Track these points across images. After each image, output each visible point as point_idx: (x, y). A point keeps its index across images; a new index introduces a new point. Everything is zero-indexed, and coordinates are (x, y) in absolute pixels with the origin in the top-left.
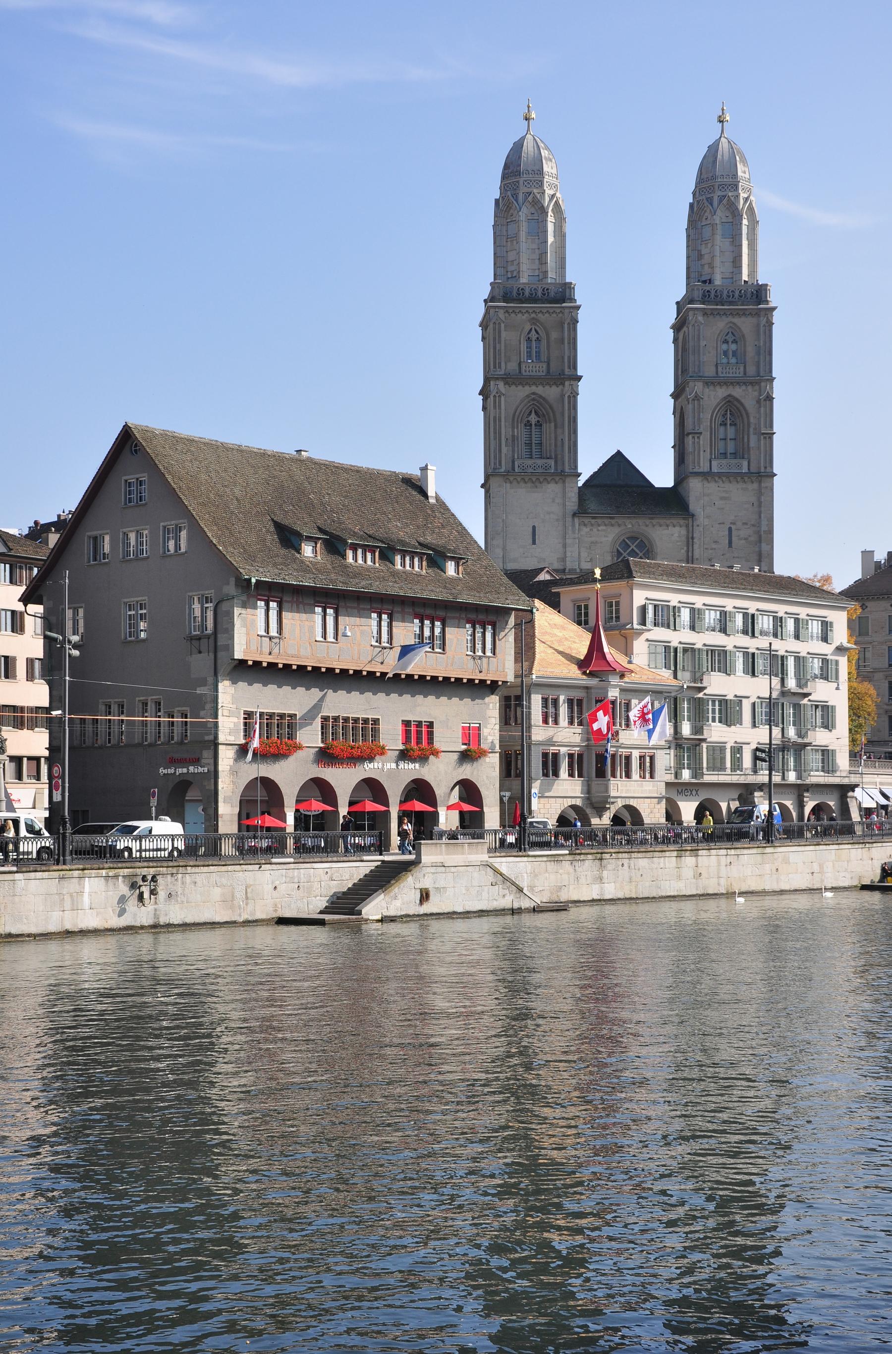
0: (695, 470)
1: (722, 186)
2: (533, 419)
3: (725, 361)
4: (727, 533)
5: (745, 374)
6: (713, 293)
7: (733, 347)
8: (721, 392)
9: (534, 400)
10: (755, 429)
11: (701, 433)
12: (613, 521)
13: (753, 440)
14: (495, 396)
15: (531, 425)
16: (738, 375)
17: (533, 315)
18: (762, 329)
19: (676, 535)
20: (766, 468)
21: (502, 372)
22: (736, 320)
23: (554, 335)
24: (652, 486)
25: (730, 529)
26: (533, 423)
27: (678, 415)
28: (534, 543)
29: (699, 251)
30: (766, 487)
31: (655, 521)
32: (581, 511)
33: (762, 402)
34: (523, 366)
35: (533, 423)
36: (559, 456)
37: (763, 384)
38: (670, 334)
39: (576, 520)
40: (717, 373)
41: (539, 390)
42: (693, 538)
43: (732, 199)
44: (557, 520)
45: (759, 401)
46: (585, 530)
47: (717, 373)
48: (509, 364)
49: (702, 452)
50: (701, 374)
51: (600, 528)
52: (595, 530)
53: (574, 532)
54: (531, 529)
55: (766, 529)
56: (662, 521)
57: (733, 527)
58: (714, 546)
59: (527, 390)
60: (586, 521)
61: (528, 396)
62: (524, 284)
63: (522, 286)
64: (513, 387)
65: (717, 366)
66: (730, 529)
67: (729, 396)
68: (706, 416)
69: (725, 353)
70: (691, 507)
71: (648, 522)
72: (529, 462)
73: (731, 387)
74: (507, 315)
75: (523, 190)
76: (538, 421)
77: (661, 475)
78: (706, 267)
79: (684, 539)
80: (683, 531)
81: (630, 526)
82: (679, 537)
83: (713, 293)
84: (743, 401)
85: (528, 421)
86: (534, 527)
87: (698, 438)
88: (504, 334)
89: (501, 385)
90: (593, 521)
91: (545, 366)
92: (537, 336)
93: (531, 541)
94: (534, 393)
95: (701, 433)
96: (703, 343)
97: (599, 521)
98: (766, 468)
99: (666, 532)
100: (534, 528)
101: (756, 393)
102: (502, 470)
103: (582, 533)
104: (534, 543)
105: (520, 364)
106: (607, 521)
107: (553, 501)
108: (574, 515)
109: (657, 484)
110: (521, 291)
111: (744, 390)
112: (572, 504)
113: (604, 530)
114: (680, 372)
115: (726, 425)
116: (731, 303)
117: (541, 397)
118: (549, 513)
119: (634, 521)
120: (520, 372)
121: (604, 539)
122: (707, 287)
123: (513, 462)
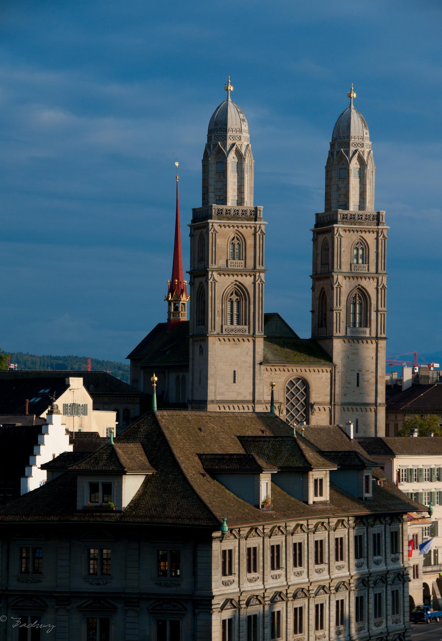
0: (337, 335)
1: (356, 145)
2: (234, 297)
3: (355, 261)
4: (356, 377)
5: (368, 270)
6: (349, 216)
7: (360, 252)
8: (354, 283)
9: (235, 285)
10: (374, 308)
11: (341, 310)
12: (286, 369)
13: (373, 315)
14: (212, 283)
15: (232, 302)
16: (364, 272)
17: (236, 228)
18: (380, 241)
19: (324, 378)
20: (381, 333)
21: (216, 267)
22: (363, 235)
23: (250, 242)
24: (297, 337)
25: (358, 374)
26: (234, 300)
27: (318, 292)
28: (234, 382)
29: (338, 185)
30: (381, 347)
31: (312, 369)
32: (265, 362)
33: (380, 291)
34: (229, 262)
35: (234, 300)
36: (252, 324)
37: (380, 279)
38: (311, 235)
39: (263, 367)
40: (351, 270)
41: (240, 279)
42: (335, 380)
43: (361, 153)
44: (250, 367)
45: (377, 289)
46: (267, 374)
47: (351, 270)
48: (220, 260)
49: (341, 323)
50: (341, 271)
51: (277, 373)
52: (273, 374)
53: (260, 375)
54: (233, 373)
55: (381, 375)
56: (316, 369)
57: (360, 373)
58: (348, 386)
59: (232, 279)
60: (268, 368)
61: (232, 283)
62: (230, 207)
63: (229, 208)
64: (223, 276)
65: (351, 265)
66: (358, 374)
67: (359, 285)
68: (344, 299)
69: (357, 257)
70: (334, 360)
71: (307, 369)
72: (233, 327)
73: (360, 279)
74: (219, 227)
75: (229, 142)
76: (237, 299)
77: (304, 332)
78: (342, 196)
79: (329, 380)
80: (329, 375)
81: (295, 371)
82: (326, 379)
83: (349, 216)
84: (367, 289)
85: (231, 299)
86: (235, 371)
87: (340, 313)
88: (218, 240)
89: (215, 274)
90: (273, 368)
91: (243, 262)
92: (238, 242)
93: (232, 381)
94: (236, 281)
95: (341, 310)
96: (343, 249)
97: (277, 368)
98: (381, 333)
99: (318, 376)
100: (235, 371)
101: (376, 284)
102: (215, 333)
103: (265, 376)
104: (234, 382)
105: (227, 261)
106: (282, 368)
107: (247, 354)
108: (261, 364)
109: (301, 338)
110: (228, 211)
111: (367, 282)
112: (260, 356)
113: (278, 374)
114: (319, 262)
115: (355, 304)
116: (360, 224)
117: (240, 283)
118: (244, 362)
119: (299, 369)
120: (227, 266)
121: (279, 380)
122: (345, 212)
123: (222, 327)
